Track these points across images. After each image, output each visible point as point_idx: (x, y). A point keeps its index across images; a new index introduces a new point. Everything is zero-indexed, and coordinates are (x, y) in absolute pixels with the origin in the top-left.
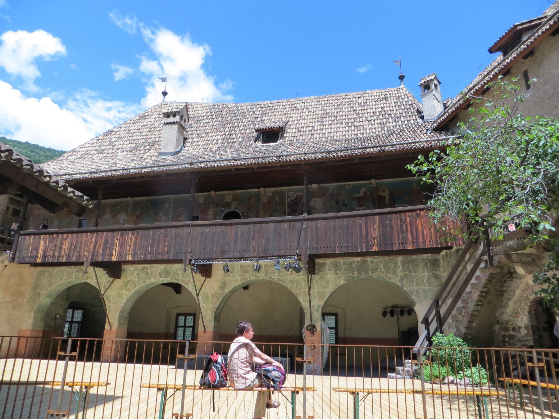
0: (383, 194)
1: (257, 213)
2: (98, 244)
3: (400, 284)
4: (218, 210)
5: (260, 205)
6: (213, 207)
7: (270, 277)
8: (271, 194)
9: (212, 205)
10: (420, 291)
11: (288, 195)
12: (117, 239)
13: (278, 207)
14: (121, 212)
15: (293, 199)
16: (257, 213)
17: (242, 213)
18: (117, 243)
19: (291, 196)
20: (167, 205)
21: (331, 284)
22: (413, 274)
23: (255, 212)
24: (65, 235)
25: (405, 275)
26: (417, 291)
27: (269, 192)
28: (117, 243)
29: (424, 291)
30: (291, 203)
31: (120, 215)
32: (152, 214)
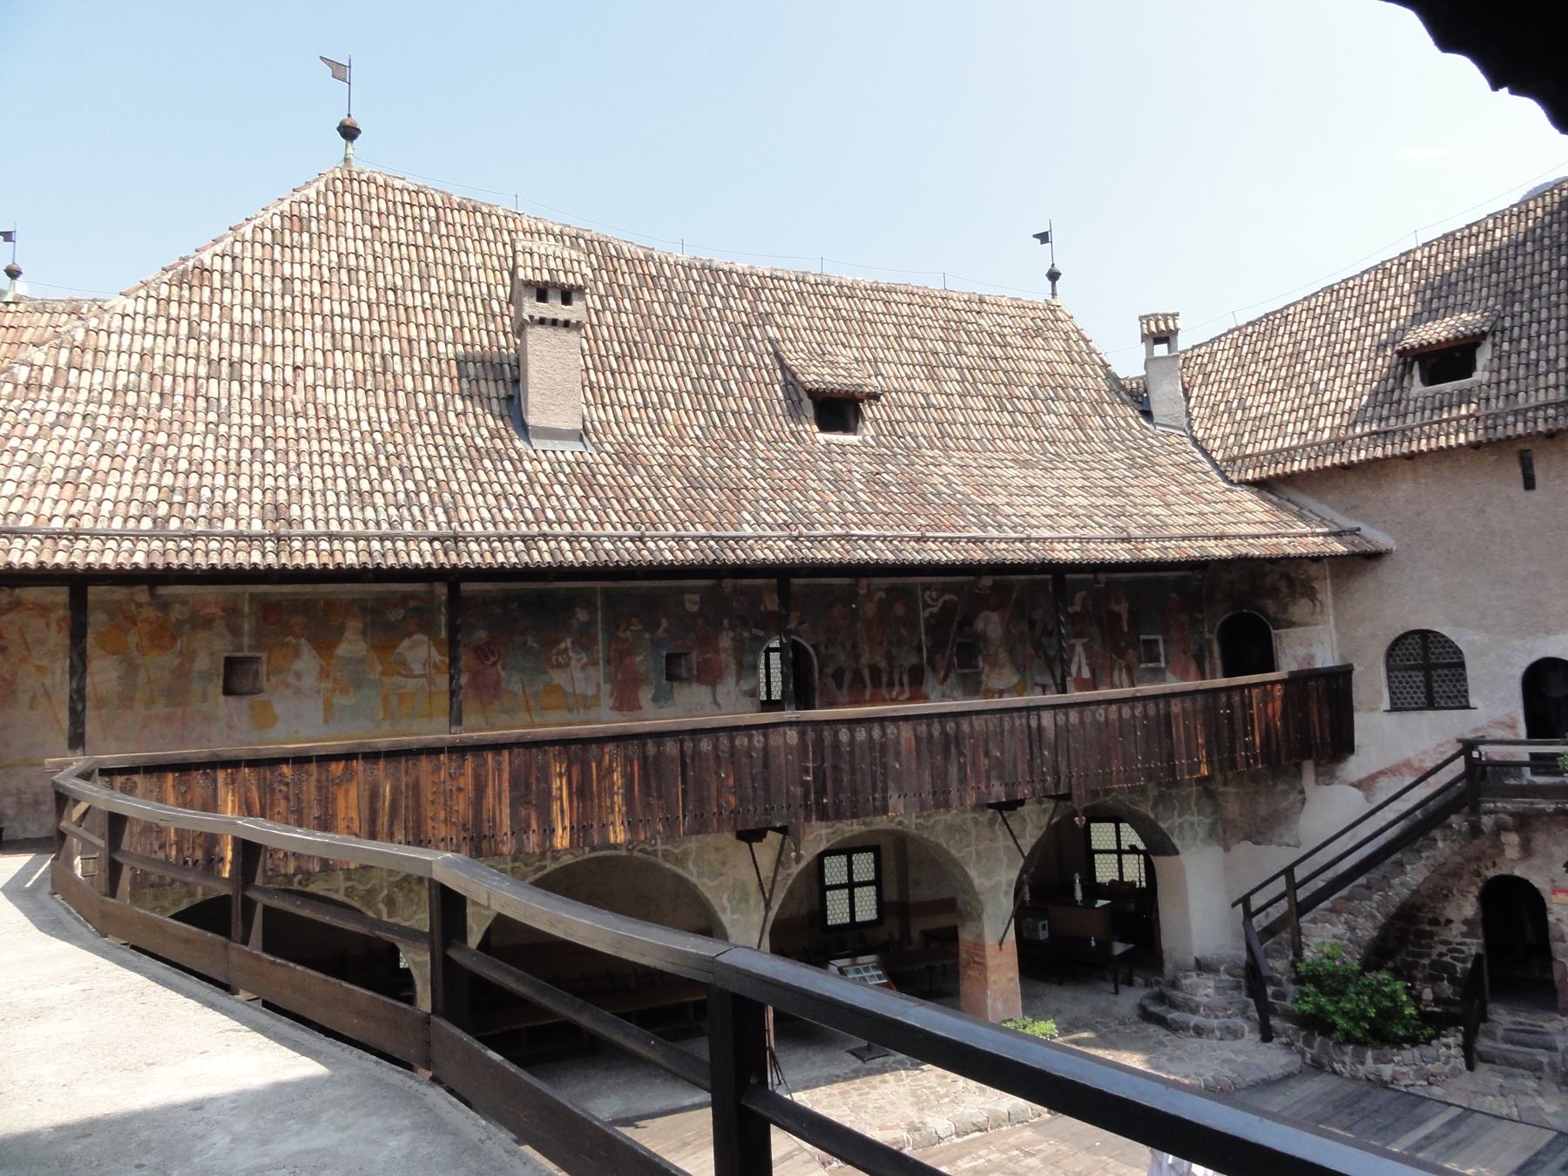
0: (1116, 608)
1: (854, 646)
2: (490, 792)
3: (1152, 816)
4: (746, 634)
5: (859, 625)
6: (732, 628)
7: (900, 823)
8: (882, 594)
9: (726, 621)
10: (1186, 826)
11: (924, 601)
12: (560, 775)
13: (904, 632)
14: (410, 635)
15: (935, 610)
16: (854, 646)
17: (814, 647)
18: (560, 786)
20: (582, 616)
21: (1030, 827)
22: (1173, 791)
23: (849, 644)
24: (337, 768)
25: (1161, 795)
26: (1181, 825)
27: (880, 589)
28: (560, 786)
29: (1192, 825)
30: (932, 621)
31: (406, 642)
32: (531, 641)
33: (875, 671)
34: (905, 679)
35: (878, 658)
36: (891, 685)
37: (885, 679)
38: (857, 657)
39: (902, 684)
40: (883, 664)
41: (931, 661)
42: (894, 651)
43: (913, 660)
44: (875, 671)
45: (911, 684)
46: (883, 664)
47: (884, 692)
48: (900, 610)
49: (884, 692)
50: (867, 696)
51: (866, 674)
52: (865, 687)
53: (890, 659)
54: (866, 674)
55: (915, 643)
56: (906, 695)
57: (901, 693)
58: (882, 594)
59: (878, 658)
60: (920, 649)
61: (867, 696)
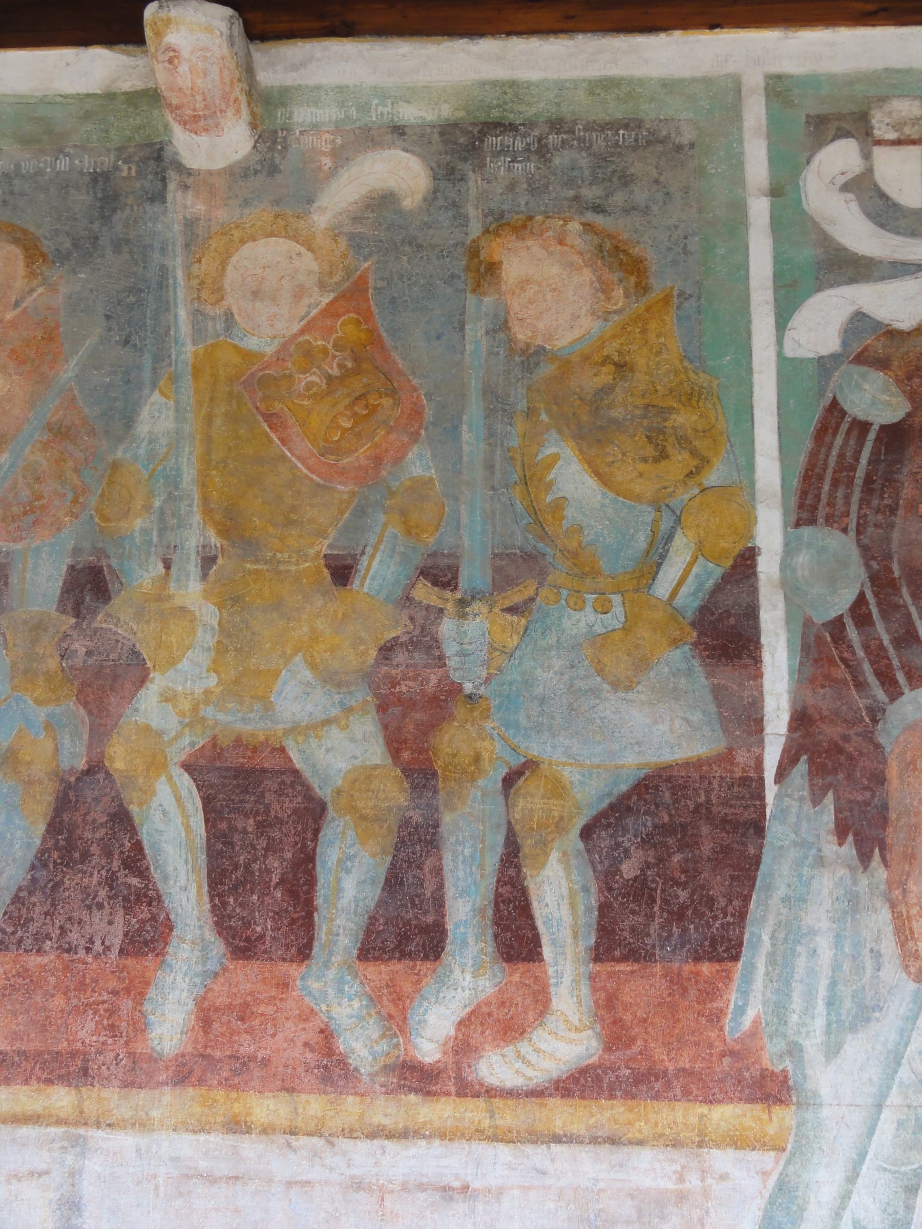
1: (89, 585)
5: (157, 417)
8: (402, 173)
13: (572, 480)
16: (89, 585)
19: (858, 234)
33: (260, 815)
34: (560, 895)
35: (296, 698)
36: (406, 935)
37: (349, 881)
38: (105, 683)
39: (515, 935)
40: (343, 752)
41: (832, 750)
42: (468, 637)
43: (657, 726)
44: (260, 815)
45: (612, 942)
46: (343, 752)
47: (335, 992)
48: (552, 294)
49: (335, 992)
50: (169, 1021)
51: (173, 828)
52: (149, 937)
53: (419, 721)
54: (173, 828)
55: (684, 576)
56: (564, 1039)
57: (503, 1022)
58: (402, 173)
59: (296, 698)
60: (726, 637)
61: (169, 1021)
